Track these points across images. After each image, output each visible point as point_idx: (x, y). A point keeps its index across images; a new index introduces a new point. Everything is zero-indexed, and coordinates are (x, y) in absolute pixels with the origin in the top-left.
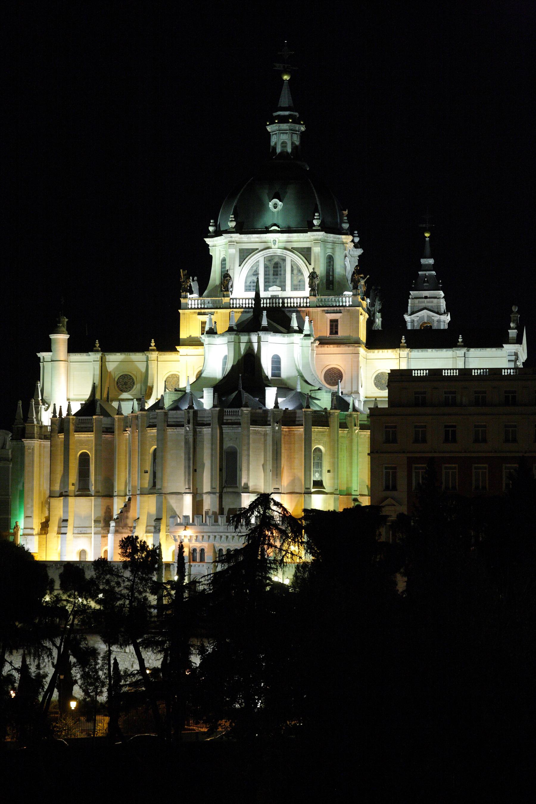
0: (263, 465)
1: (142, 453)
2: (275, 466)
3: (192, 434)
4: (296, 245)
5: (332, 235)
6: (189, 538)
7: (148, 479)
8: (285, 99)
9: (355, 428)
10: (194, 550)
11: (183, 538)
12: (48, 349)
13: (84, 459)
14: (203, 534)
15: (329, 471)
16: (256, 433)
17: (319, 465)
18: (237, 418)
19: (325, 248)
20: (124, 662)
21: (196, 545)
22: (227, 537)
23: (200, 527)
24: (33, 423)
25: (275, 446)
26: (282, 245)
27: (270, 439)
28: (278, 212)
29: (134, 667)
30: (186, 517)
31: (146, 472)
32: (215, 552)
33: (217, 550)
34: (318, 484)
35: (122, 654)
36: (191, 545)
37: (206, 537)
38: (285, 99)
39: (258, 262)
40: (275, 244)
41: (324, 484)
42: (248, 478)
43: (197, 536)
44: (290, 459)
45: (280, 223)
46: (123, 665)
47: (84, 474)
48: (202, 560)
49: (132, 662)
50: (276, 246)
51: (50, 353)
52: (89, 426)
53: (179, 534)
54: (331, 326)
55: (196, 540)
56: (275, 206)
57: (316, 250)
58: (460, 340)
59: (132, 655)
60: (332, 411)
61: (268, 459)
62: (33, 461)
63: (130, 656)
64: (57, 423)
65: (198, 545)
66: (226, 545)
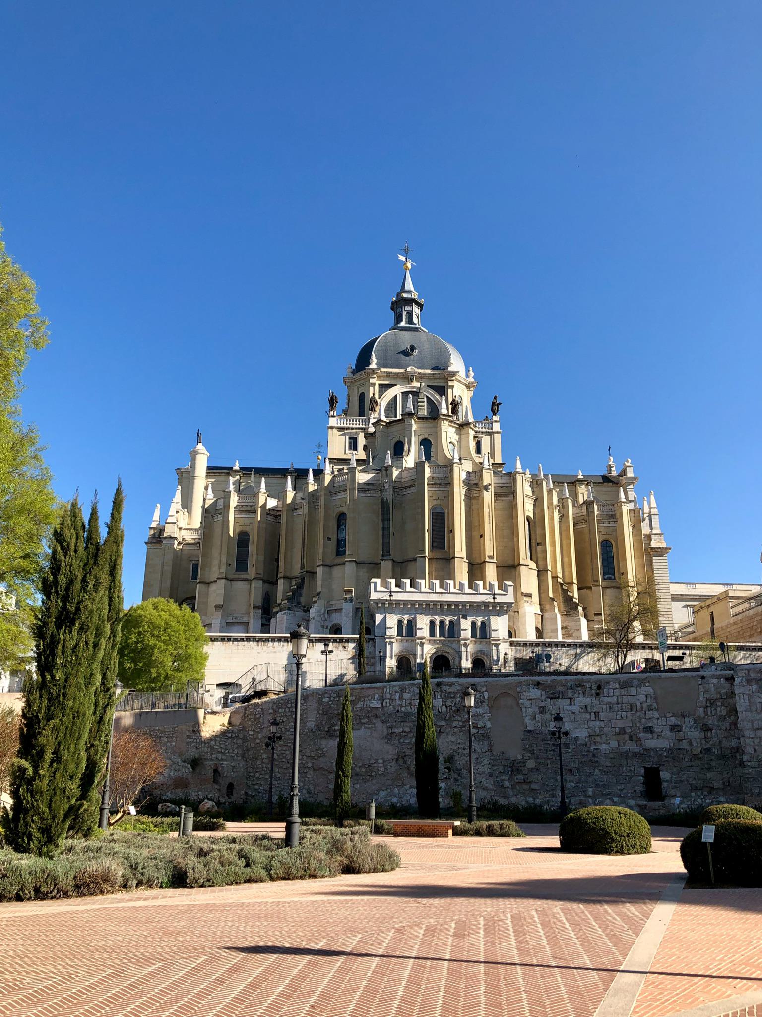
31: (329, 539)
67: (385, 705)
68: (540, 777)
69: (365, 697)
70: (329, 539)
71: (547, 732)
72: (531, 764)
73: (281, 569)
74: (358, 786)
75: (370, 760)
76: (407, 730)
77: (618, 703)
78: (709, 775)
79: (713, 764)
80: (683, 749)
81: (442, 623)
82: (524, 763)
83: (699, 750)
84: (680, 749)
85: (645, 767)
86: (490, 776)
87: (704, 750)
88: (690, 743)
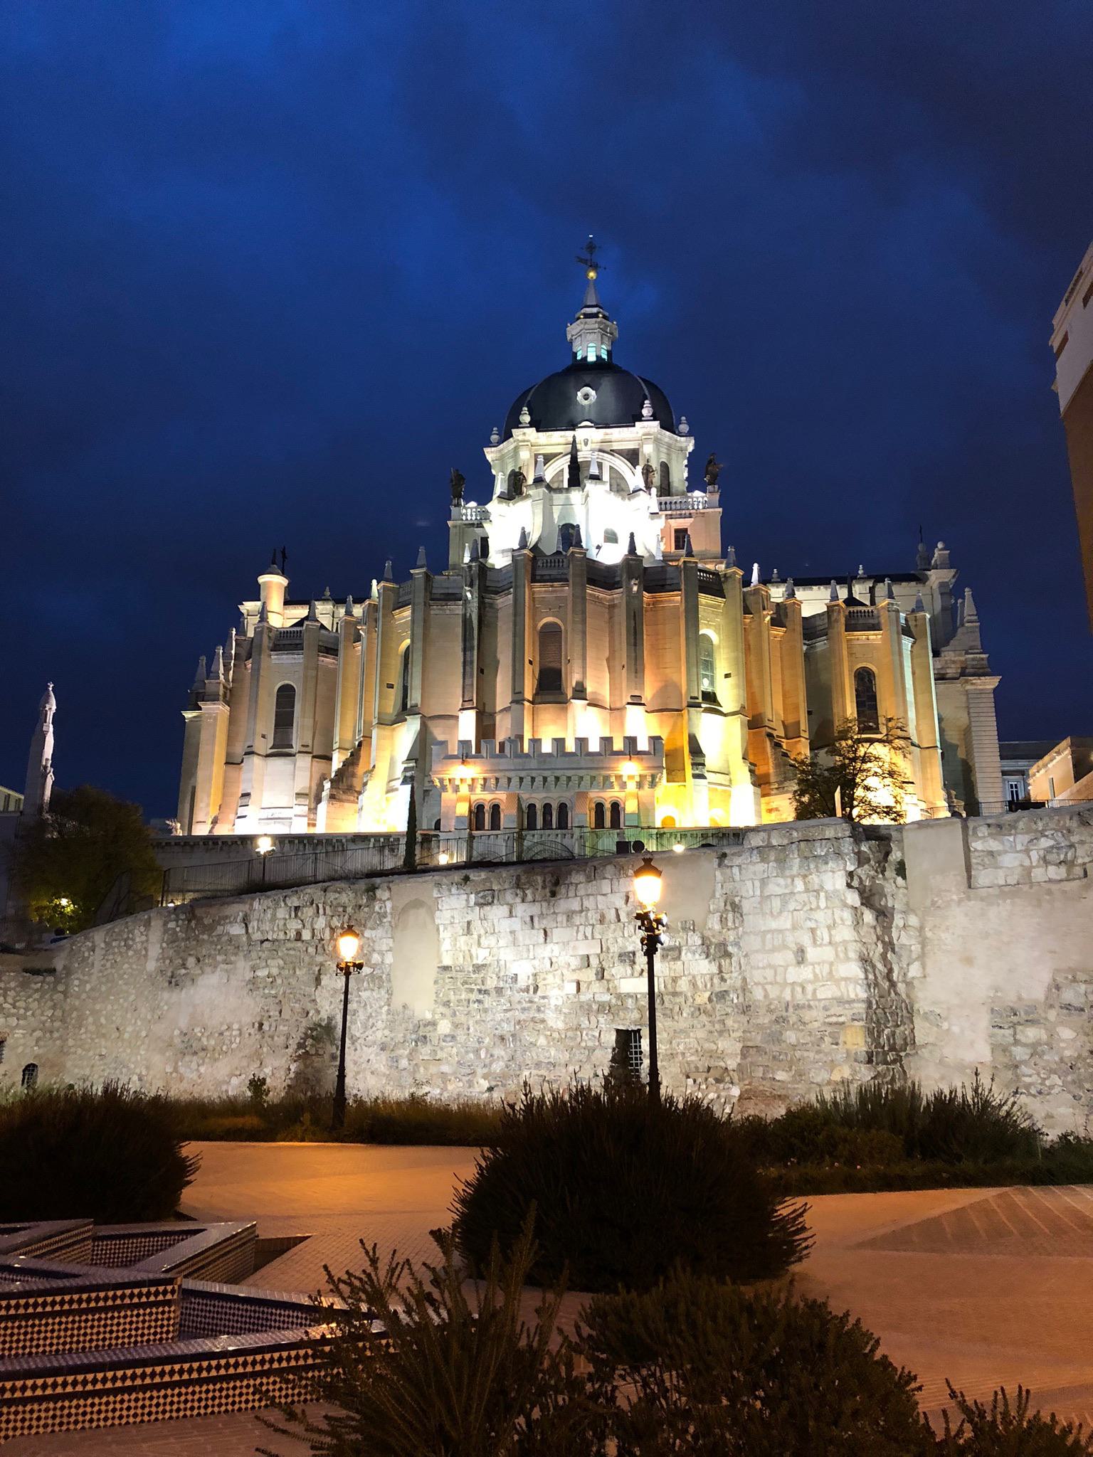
0: (608, 660)
1: (385, 653)
2: (633, 655)
3: (476, 604)
4: (616, 446)
5: (668, 433)
6: (470, 782)
7: (393, 698)
8: (592, 299)
9: (765, 612)
10: (480, 807)
11: (458, 782)
12: (256, 598)
13: (286, 696)
14: (497, 775)
15: (727, 676)
16: (597, 601)
17: (709, 665)
18: (561, 571)
19: (658, 450)
20: (294, 969)
21: (482, 796)
22: (545, 779)
23: (493, 760)
24: (218, 678)
25: (633, 622)
26: (597, 446)
27: (621, 616)
28: (590, 405)
29: (323, 983)
30: (465, 744)
31: (391, 686)
32: (520, 808)
33: (524, 806)
34: (710, 697)
35: (289, 945)
36: (473, 798)
37: (503, 781)
38: (592, 299)
39: (562, 470)
40: (586, 444)
41: (719, 698)
42: (584, 673)
43: (485, 779)
44: (657, 651)
45: (593, 417)
46: (291, 980)
47: (284, 721)
48: (495, 825)
49: (317, 969)
50: (589, 447)
51: (259, 604)
52: (298, 642)
53: (451, 777)
54: (677, 539)
55: (484, 787)
56: (586, 397)
57: (648, 449)
58: (861, 572)
59: (320, 946)
60: (729, 571)
61: (617, 648)
62: (214, 736)
63: (311, 950)
64: (246, 646)
65: (486, 797)
66: (544, 795)
67: (250, 931)
68: (455, 1050)
69: (227, 917)
70: (391, 686)
71: (471, 969)
72: (444, 1027)
73: (337, 739)
74: (202, 1069)
75: (222, 1024)
76: (275, 971)
77: (581, 911)
78: (722, 1044)
79: (729, 1022)
80: (681, 993)
81: (547, 807)
82: (433, 1024)
83: (707, 994)
84: (675, 994)
85: (618, 1031)
86: (383, 1049)
87: (717, 995)
88: (694, 984)
